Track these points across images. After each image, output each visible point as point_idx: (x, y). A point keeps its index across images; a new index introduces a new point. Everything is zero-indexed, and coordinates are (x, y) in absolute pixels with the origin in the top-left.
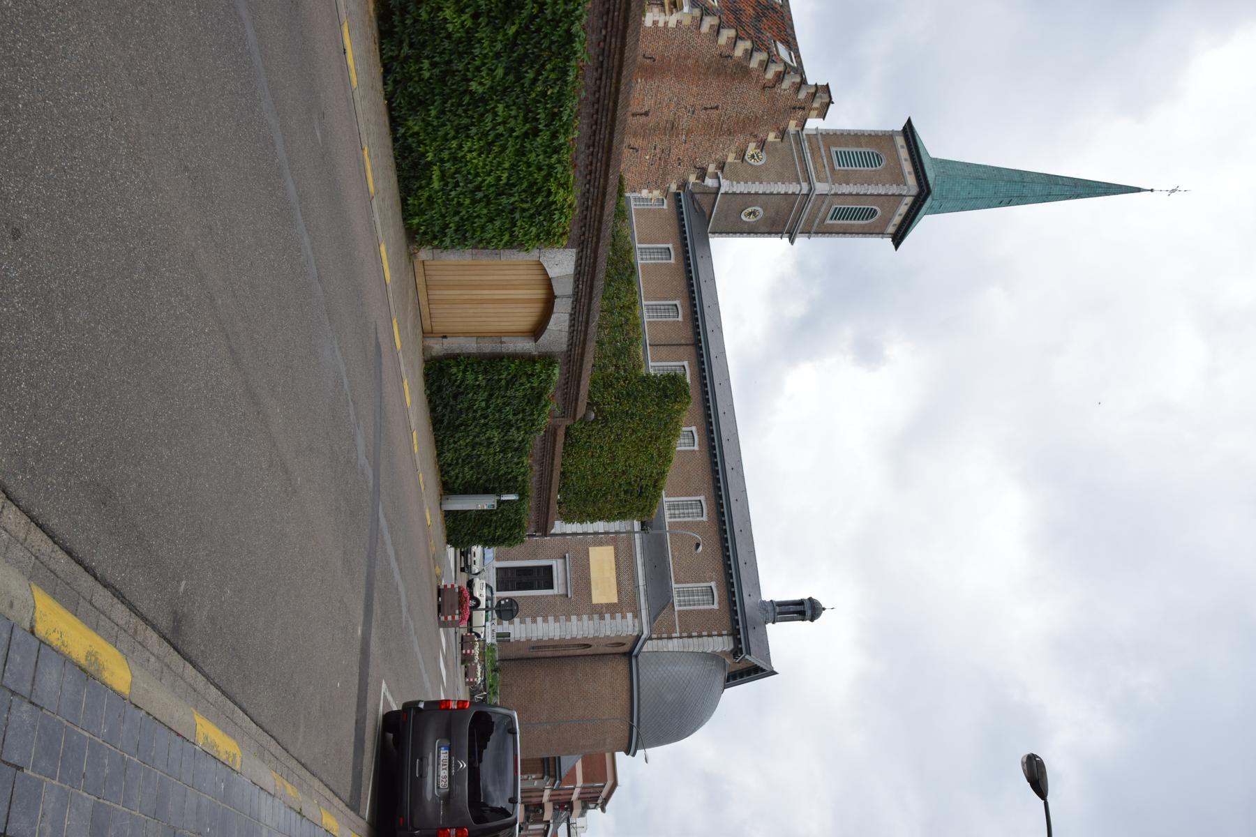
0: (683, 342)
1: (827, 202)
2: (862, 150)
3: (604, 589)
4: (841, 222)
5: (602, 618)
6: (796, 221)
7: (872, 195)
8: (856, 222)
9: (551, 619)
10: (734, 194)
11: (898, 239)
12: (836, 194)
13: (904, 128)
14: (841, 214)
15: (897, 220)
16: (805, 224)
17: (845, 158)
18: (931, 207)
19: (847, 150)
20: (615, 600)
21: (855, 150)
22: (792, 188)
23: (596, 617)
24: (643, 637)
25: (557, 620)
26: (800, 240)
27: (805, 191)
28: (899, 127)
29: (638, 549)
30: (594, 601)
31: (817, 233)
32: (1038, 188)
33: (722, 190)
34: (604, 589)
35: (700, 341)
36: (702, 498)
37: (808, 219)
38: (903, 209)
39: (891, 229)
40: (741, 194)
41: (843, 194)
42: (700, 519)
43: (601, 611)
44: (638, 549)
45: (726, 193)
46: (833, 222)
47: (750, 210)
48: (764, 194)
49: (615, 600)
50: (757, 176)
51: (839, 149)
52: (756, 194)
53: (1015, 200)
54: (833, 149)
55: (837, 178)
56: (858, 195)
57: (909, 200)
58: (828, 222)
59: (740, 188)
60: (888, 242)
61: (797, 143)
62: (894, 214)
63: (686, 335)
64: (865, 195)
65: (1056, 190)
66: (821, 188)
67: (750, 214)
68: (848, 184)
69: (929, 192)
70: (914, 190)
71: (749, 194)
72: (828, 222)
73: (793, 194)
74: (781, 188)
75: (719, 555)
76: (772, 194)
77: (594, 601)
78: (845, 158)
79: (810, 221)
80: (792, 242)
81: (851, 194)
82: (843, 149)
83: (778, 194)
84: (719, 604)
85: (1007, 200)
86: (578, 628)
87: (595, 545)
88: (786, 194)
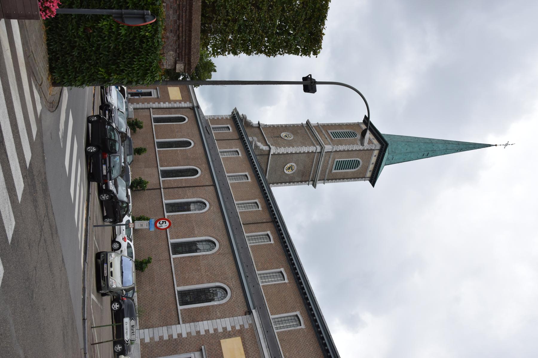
0: (264, 221)
1: (331, 157)
2: (345, 131)
4: (340, 171)
6: (316, 172)
7: (356, 150)
8: (349, 170)
10: (279, 154)
11: (373, 180)
12: (336, 151)
13: (364, 121)
14: (341, 165)
15: (371, 167)
16: (321, 174)
17: (336, 135)
18: (388, 159)
19: (336, 131)
21: (341, 131)
22: (312, 149)
26: (320, 185)
27: (319, 150)
28: (361, 121)
29: (261, 336)
31: (328, 180)
32: (441, 146)
33: (272, 153)
35: (276, 218)
36: (298, 313)
37: (322, 170)
38: (374, 160)
39: (369, 174)
40: (283, 154)
41: (340, 151)
42: (299, 327)
44: (261, 336)
45: (274, 154)
46: (336, 171)
47: (289, 165)
48: (296, 153)
50: (290, 144)
51: (332, 131)
52: (292, 153)
53: (430, 153)
54: (329, 131)
55: (333, 143)
56: (348, 151)
57: (376, 153)
58: (334, 171)
59: (282, 150)
60: (368, 183)
61: (308, 130)
62: (369, 164)
63: (266, 217)
64: (352, 150)
65: (450, 147)
66: (328, 148)
67: (289, 168)
68: (341, 145)
69: (387, 145)
70: (378, 146)
71: (287, 154)
72: (334, 171)
73: (312, 152)
74: (305, 149)
75: (320, 351)
76: (300, 153)
78: (336, 135)
79: (324, 171)
80: (314, 186)
81: (344, 151)
82: (334, 131)
83: (304, 153)
85: (426, 153)
87: (225, 338)
88: (308, 152)
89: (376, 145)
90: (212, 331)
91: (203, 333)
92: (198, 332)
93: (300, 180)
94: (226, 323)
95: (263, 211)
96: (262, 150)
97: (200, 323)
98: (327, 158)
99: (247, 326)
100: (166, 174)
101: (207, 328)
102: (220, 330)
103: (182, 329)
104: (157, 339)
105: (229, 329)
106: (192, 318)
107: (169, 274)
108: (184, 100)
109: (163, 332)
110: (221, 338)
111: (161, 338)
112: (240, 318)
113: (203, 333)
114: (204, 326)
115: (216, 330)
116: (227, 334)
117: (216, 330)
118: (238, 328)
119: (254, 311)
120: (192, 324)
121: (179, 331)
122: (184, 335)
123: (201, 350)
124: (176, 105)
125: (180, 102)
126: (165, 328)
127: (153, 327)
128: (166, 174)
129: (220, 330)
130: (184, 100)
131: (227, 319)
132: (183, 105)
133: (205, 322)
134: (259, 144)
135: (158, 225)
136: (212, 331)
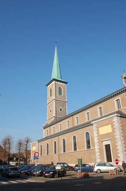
3: (106, 130)
5: (115, 128)
9: (117, 144)
20: (110, 125)
22: (54, 103)
23: (115, 130)
24: (119, 115)
25: (117, 143)
27: (55, 101)
30: (111, 131)
33: (55, 116)
34: (106, 130)
38: (59, 83)
43: (113, 129)
49: (110, 125)
57: (56, 82)
66: (54, 97)
69: (54, 79)
77: (111, 131)
84: (118, 97)
86: (118, 135)
89: (54, 82)
90: (97, 138)
91: (98, 141)
92: (98, 142)
93: (65, 107)
94: (95, 133)
95: (70, 119)
96: (54, 119)
97: (95, 141)
98: (57, 98)
99: (96, 126)
100: (55, 152)
101: (96, 140)
102: (97, 135)
103: (97, 147)
104: (99, 157)
105: (97, 132)
106: (94, 145)
107: (82, 152)
108: (36, 145)
109: (98, 154)
110: (99, 134)
111: (99, 155)
112: (94, 128)
113: (98, 141)
114: (96, 141)
115: (97, 136)
116: (98, 133)
117: (97, 136)
118: (96, 129)
119: (92, 123)
120: (95, 144)
121: (97, 149)
122: (98, 147)
123: (102, 141)
124: (37, 148)
125: (36, 147)
126: (96, 154)
127: (96, 158)
128: (55, 152)
129: (97, 135)
130: (36, 145)
131: (94, 132)
132: (37, 146)
133: (95, 140)
134: (52, 120)
135: (36, 156)
136: (97, 138)
